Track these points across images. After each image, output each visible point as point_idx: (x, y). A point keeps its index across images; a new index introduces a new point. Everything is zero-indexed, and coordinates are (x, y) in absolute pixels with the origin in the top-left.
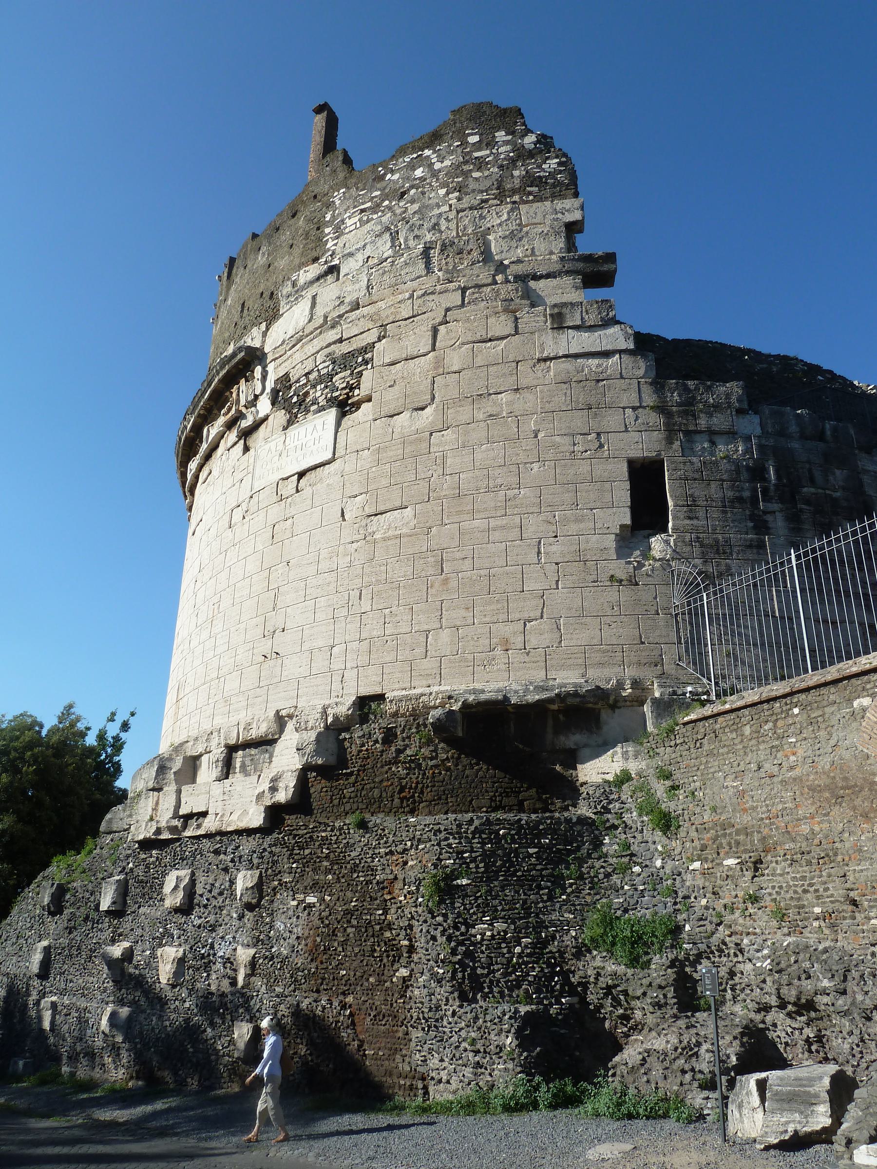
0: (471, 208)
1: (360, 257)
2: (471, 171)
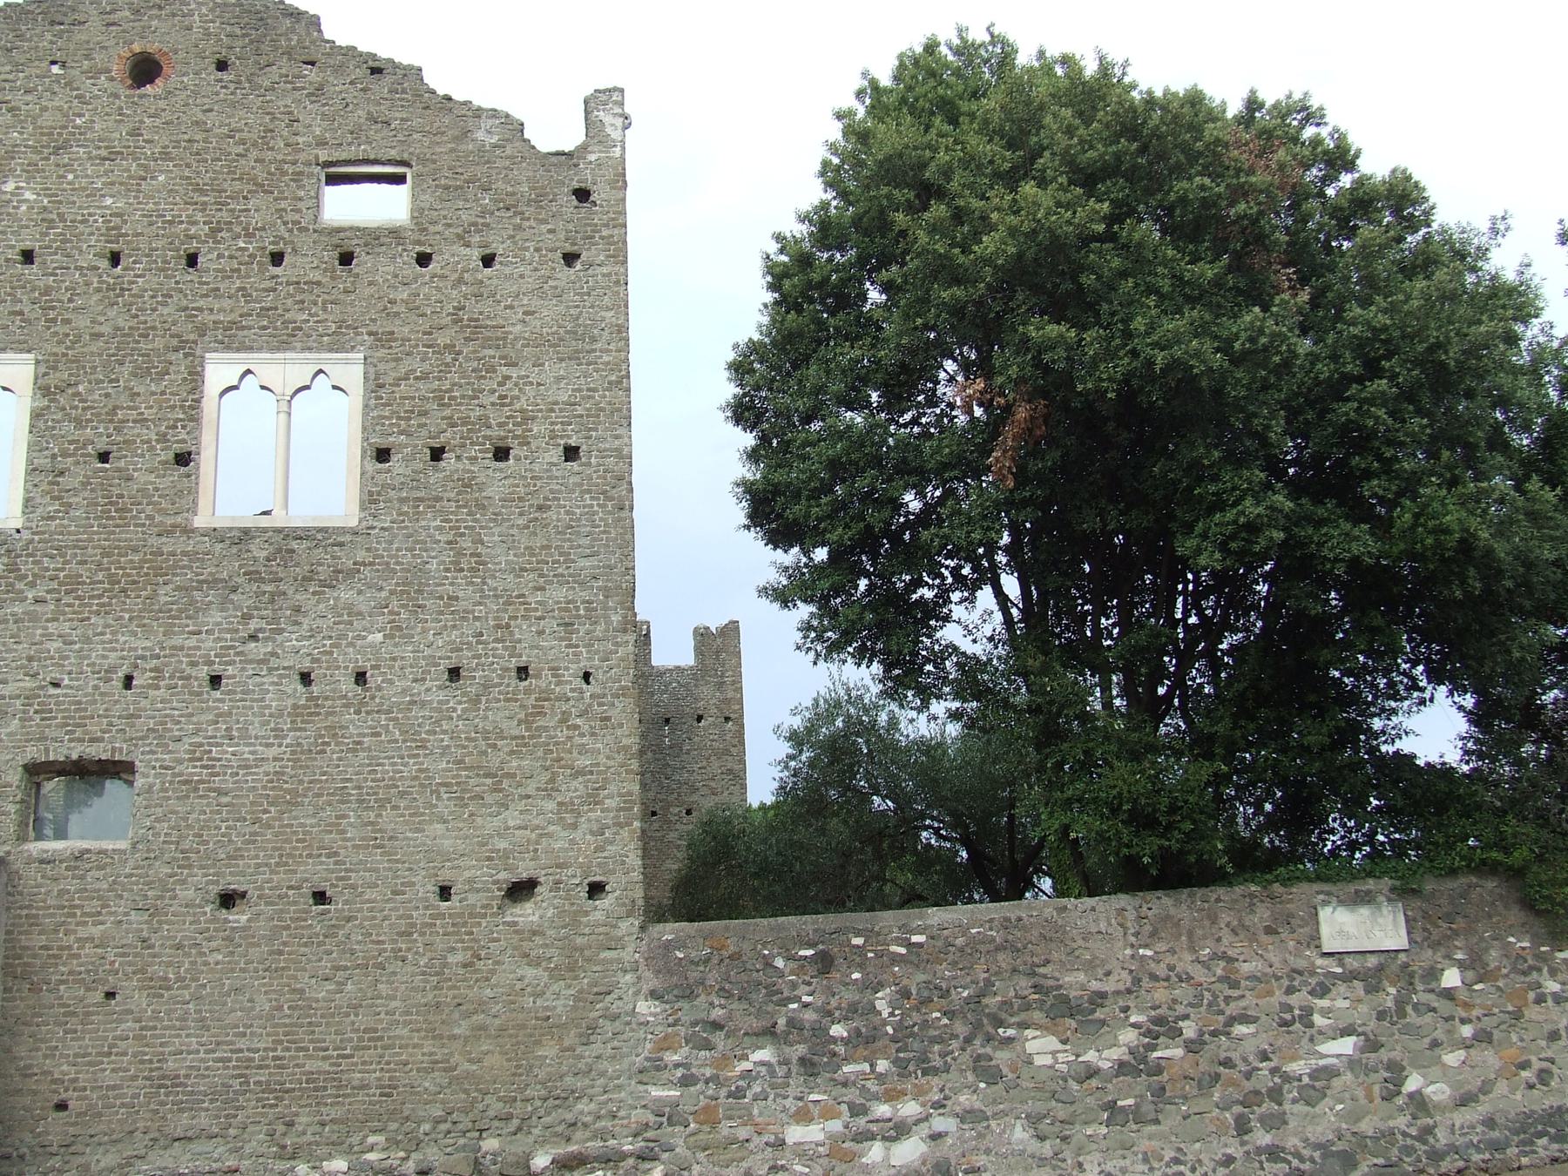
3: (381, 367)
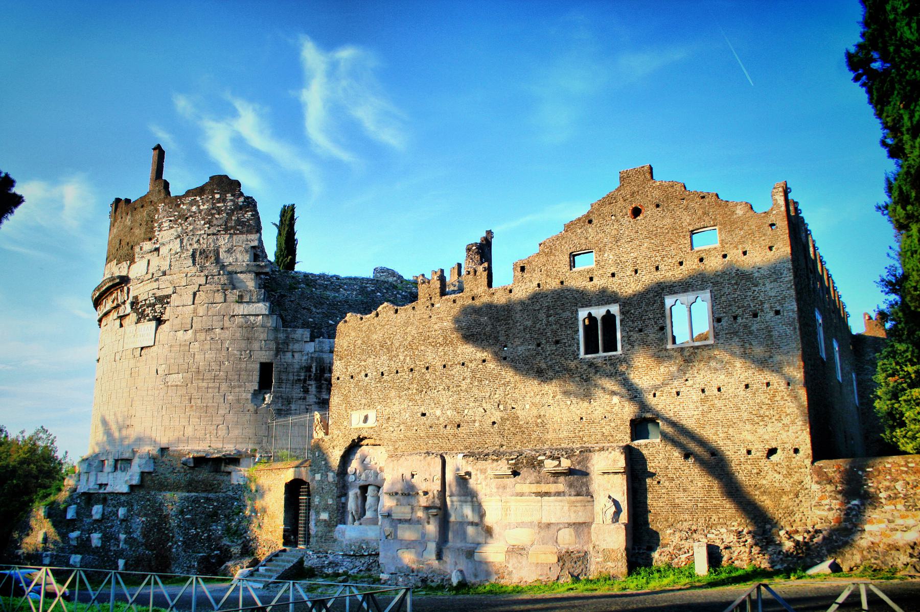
0: (214, 234)
1: (167, 248)
2: (215, 214)
3: (716, 293)
